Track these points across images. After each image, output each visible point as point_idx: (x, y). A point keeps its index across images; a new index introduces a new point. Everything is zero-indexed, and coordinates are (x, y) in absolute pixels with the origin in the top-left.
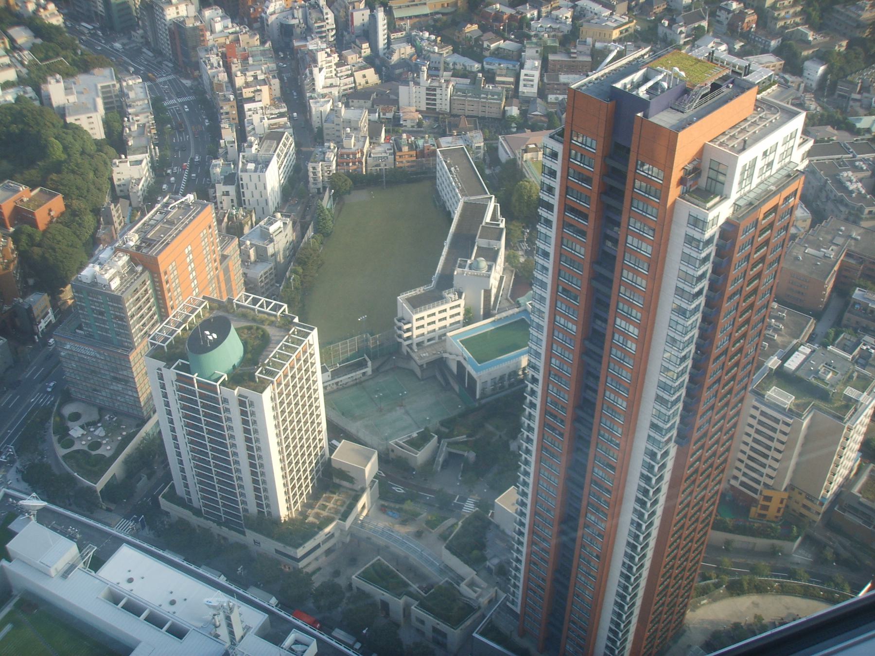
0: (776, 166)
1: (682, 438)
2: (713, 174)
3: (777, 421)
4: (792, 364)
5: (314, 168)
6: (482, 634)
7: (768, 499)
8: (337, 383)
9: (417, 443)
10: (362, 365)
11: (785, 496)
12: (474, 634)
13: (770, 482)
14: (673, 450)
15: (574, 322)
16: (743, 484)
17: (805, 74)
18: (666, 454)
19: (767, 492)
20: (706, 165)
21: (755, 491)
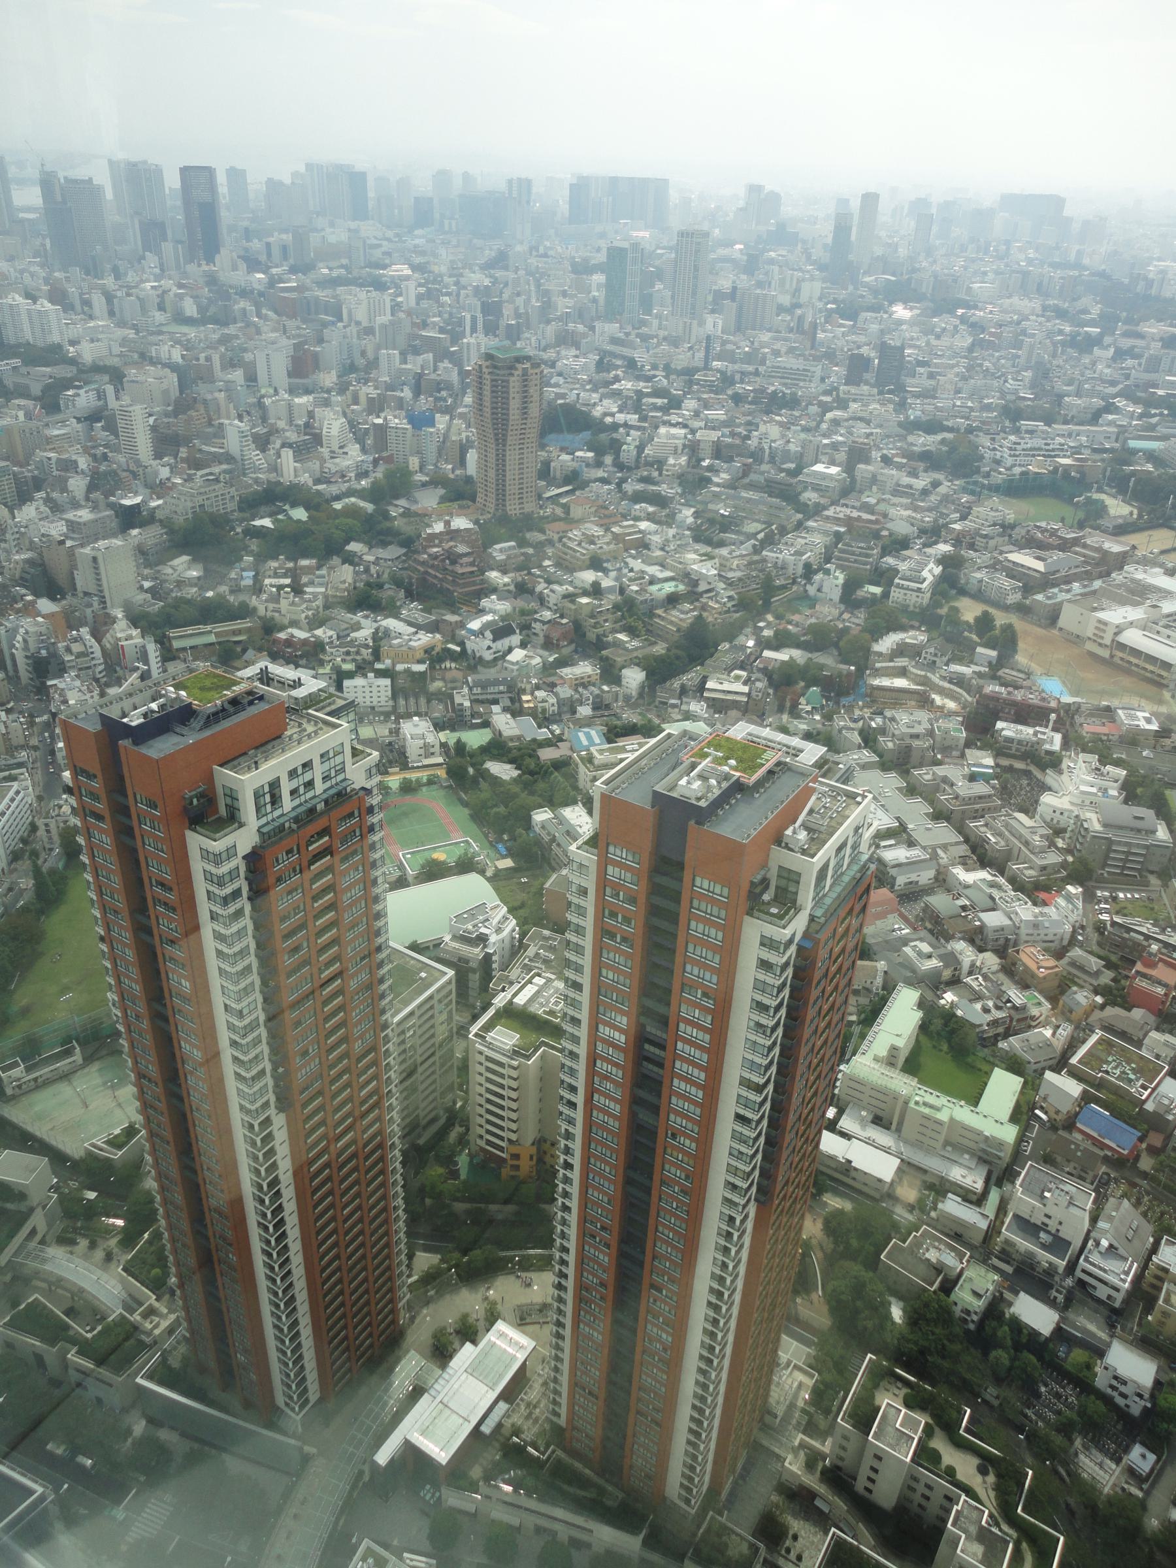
0: (320, 787)
1: (284, 1103)
2: (229, 801)
3: (501, 1065)
4: (520, 1000)
5: (47, 825)
6: (150, 1377)
7: (516, 1157)
8: (35, 1080)
9: (115, 1143)
10: (68, 1053)
11: (534, 1151)
12: (139, 1380)
13: (514, 1137)
14: (279, 1121)
15: (137, 982)
16: (489, 1142)
17: (624, 682)
18: (267, 1122)
19: (514, 1150)
20: (220, 791)
21: (501, 1149)
